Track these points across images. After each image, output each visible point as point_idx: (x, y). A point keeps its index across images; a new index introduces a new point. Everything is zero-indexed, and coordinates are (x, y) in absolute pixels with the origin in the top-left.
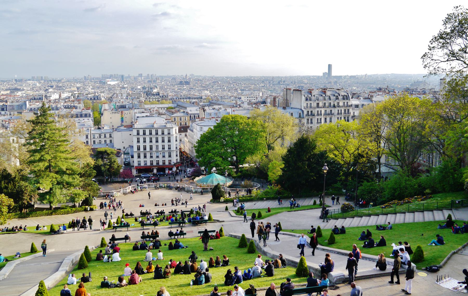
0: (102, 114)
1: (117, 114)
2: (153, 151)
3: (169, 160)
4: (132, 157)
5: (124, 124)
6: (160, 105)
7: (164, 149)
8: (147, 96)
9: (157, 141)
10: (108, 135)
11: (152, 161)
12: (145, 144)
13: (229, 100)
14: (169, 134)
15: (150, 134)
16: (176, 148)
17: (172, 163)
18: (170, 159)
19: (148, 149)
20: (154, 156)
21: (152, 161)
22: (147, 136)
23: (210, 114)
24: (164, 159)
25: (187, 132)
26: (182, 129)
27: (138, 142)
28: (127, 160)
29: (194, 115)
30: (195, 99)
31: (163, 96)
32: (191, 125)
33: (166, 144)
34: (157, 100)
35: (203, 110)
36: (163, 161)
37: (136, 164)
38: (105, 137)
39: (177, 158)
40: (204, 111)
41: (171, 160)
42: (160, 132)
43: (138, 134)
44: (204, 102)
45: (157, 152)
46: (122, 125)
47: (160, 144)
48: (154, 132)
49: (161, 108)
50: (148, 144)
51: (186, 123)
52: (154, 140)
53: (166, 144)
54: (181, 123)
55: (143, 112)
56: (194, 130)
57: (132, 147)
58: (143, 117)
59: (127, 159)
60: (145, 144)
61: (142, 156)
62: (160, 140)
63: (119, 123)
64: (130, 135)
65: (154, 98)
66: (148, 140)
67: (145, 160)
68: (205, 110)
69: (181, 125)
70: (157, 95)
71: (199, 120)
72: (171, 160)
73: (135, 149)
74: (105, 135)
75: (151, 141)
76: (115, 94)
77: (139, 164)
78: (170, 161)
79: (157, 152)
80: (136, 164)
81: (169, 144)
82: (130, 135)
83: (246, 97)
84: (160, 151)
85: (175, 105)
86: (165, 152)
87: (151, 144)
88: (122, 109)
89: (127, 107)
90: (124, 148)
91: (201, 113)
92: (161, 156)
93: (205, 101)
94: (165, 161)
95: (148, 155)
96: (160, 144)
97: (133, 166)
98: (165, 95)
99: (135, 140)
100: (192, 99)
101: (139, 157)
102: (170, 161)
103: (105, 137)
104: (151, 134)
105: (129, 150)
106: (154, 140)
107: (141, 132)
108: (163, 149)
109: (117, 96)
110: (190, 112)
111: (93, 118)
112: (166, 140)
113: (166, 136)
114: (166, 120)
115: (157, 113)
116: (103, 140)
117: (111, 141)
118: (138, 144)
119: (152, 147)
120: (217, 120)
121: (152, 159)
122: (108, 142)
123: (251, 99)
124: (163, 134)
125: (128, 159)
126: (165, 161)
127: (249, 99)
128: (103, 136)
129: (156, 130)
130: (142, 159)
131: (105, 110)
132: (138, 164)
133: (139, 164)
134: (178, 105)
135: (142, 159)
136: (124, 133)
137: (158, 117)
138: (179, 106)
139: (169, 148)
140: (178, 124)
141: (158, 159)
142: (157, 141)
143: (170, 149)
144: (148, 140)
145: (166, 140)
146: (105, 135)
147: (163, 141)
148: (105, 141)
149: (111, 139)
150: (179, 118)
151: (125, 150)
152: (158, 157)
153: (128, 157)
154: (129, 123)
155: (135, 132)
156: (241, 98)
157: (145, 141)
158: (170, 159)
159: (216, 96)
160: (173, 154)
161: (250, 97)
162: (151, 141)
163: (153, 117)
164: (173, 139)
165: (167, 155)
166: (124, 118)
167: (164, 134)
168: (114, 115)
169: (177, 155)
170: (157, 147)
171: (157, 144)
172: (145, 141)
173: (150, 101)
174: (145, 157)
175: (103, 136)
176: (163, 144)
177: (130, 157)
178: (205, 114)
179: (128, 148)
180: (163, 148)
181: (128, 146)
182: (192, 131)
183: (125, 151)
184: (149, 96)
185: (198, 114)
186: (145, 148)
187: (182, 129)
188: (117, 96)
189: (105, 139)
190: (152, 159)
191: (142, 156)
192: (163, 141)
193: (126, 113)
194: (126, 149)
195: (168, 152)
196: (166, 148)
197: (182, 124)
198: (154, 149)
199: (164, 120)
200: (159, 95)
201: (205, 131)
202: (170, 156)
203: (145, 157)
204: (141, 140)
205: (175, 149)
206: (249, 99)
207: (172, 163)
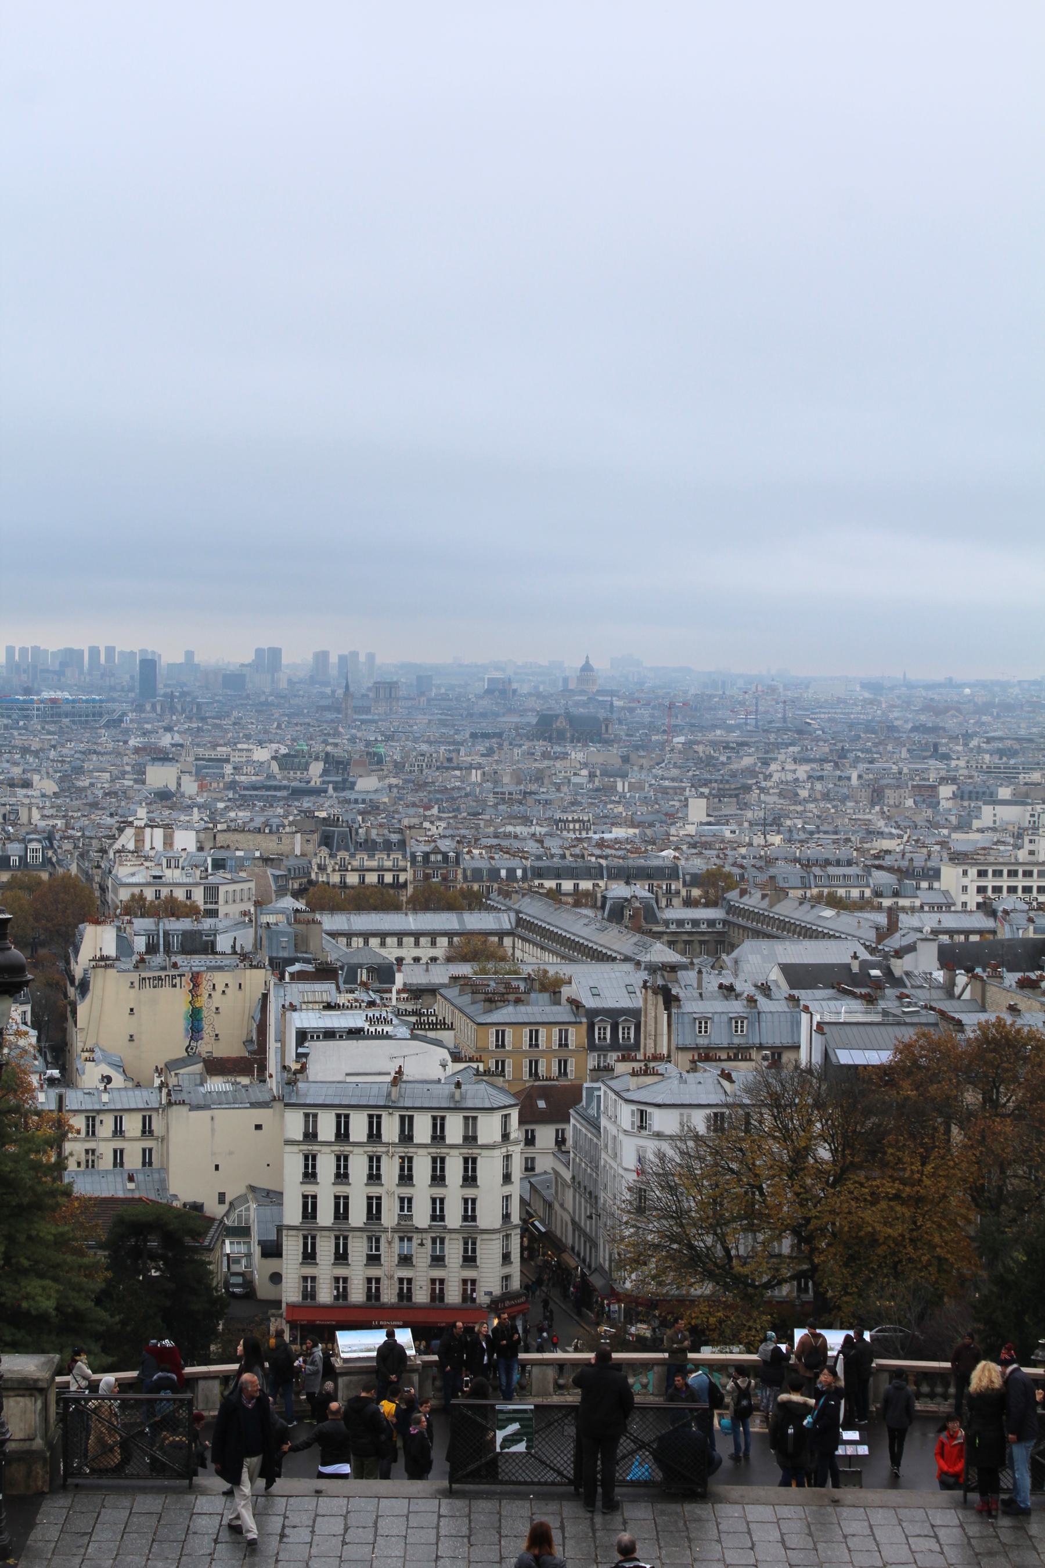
0: (84, 987)
1: (165, 992)
2: (386, 1230)
3: (465, 1282)
4: (272, 1250)
5: (205, 1047)
6: (411, 918)
7: (442, 1218)
8: (324, 851)
9: (406, 1178)
10: (132, 1125)
11: (378, 1280)
12: (341, 1190)
13: (855, 893)
14: (470, 1139)
15: (370, 1135)
16: (506, 1217)
17: (482, 1299)
18: (470, 1274)
19: (358, 1216)
20: (389, 1254)
21: (378, 1280)
22: (356, 1150)
23: (702, 1022)
24: (437, 1273)
25: (568, 1121)
26: (542, 1104)
27: (310, 1175)
28: (235, 1268)
29: (614, 1015)
30: (628, 876)
31: (426, 855)
32: (591, 1090)
33: (454, 1192)
34: (388, 878)
35: (660, 999)
36: (433, 1281)
37: (291, 1293)
38: (118, 1132)
39: (507, 1270)
40: (667, 1008)
41: (474, 1282)
42: (422, 1129)
43: (310, 1136)
44: (689, 903)
45: (406, 1232)
46: (191, 1057)
47: (422, 1190)
48: (390, 1129)
49: (417, 935)
50: (358, 1192)
51: (563, 1064)
52: (390, 1170)
53: (454, 1192)
54: (534, 1064)
55: (329, 1007)
56: (604, 1122)
57: (273, 1197)
58: (330, 1034)
59: (237, 1261)
60: (341, 1190)
61: (325, 1249)
62: (422, 1169)
63: (176, 1045)
64: (258, 1127)
65: (374, 864)
66: (358, 1167)
67: (341, 1272)
68: (677, 999)
69: (534, 1074)
70: (388, 847)
71: (634, 1074)
72: (474, 1282)
73: (292, 1214)
74: (118, 1122)
75: (374, 1177)
76: (129, 832)
77: (309, 1294)
78: (469, 1285)
79: (406, 1232)
80: (291, 1293)
81: (470, 1192)
82: (258, 1127)
83: (973, 872)
84: (418, 1230)
85: (506, 922)
86: (448, 1237)
87: (375, 1191)
88: (198, 962)
89: (223, 943)
90: (222, 1198)
91: (651, 1013)
92: (422, 1257)
93: (696, 892)
94: (442, 1281)
95: (358, 1249)
96: (422, 1190)
97: (277, 1304)
98: (436, 851)
99: (293, 1165)
100: (610, 877)
101: (309, 1256)
102: (469, 1285)
103: (118, 1132)
104: (379, 1135)
105: (253, 1213)
106: (390, 1170)
107: (327, 1127)
108: (434, 1218)
109: (139, 840)
110: (590, 1002)
111: (28, 1008)
112: (454, 1169)
113: (455, 1152)
114: (456, 1058)
115: (407, 1013)
116: (106, 1150)
117: (147, 1154)
118: (310, 1189)
119: (379, 1206)
120: (728, 1077)
121: (374, 1272)
122: (133, 1161)
123: (1005, 882)
124: (438, 1136)
125: (244, 1262)
126: (442, 1281)
127: (990, 882)
128: (106, 1128)
129: (402, 1118)
130: (325, 1269)
131: (103, 962)
132: (305, 1296)
133: (309, 1294)
134: (519, 922)
135: (325, 1269)
136: (222, 1115)
137: (414, 1037)
138: (530, 926)
139: (469, 1217)
140: (517, 1067)
141: (405, 1273)
142: (406, 1178)
143: (474, 1218)
144: (358, 1167)
145: (454, 1169)
146: (118, 1122)
147: (438, 1178)
148: (118, 1156)
149: (148, 1144)
150: (526, 1031)
151: (225, 1207)
152: (406, 1260)
153: (243, 1249)
154: (230, 1047)
155: (294, 1124)
156: (936, 874)
157: (342, 1176)
158: (470, 1274)
159: (770, 861)
160: (489, 1252)
161: (998, 874)
162: (374, 1177)
163: (387, 1037)
164: (489, 1168)
165: (454, 1251)
166: (205, 1013)
167: (443, 1138)
168: (148, 992)
169: (506, 1258)
170: (406, 1202)
171: (405, 1191)
172: (342, 1176)
173: (344, 885)
174: (341, 1257)
175: (106, 1128)
176: (438, 1192)
177: (256, 1250)
178: (674, 1017)
179: (242, 1199)
180: (438, 1216)
181: (241, 1190)
182: (594, 1125)
183: (227, 1214)
184: (342, 854)
185: (635, 1014)
186: (341, 1211)
187: (542, 1104)
188: (139, 840)
189: (119, 1144)
190: (374, 1272)
191: (325, 1249)
192: (438, 1178)
193: (220, 988)
194: (231, 1204)
195: (460, 1237)
196: (454, 1218)
197: (542, 1070)
198: (390, 1216)
199: (449, 1058)
200: (402, 844)
201: (659, 1135)
202: (469, 1259)
203: (341, 1257)
204: (326, 1166)
205: (497, 1223)
206: (990, 882)
207: (482, 1299)
